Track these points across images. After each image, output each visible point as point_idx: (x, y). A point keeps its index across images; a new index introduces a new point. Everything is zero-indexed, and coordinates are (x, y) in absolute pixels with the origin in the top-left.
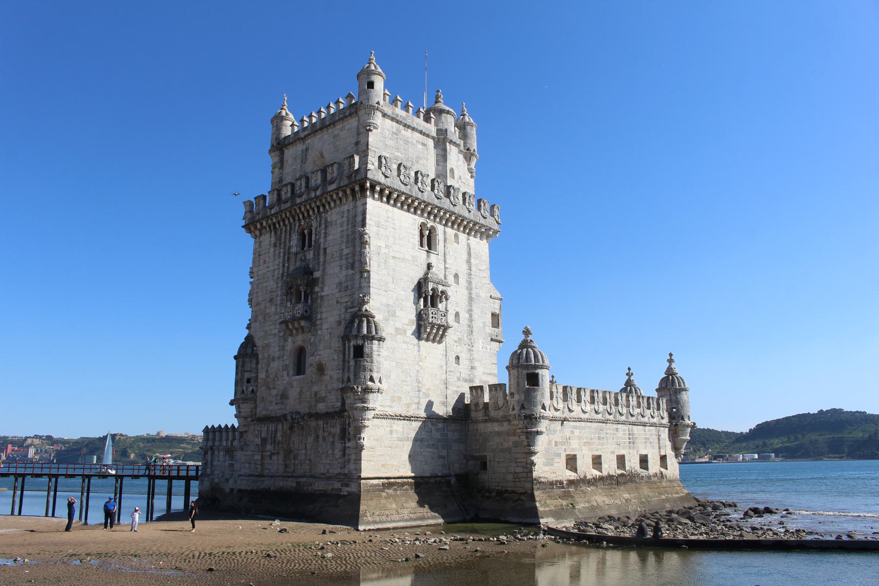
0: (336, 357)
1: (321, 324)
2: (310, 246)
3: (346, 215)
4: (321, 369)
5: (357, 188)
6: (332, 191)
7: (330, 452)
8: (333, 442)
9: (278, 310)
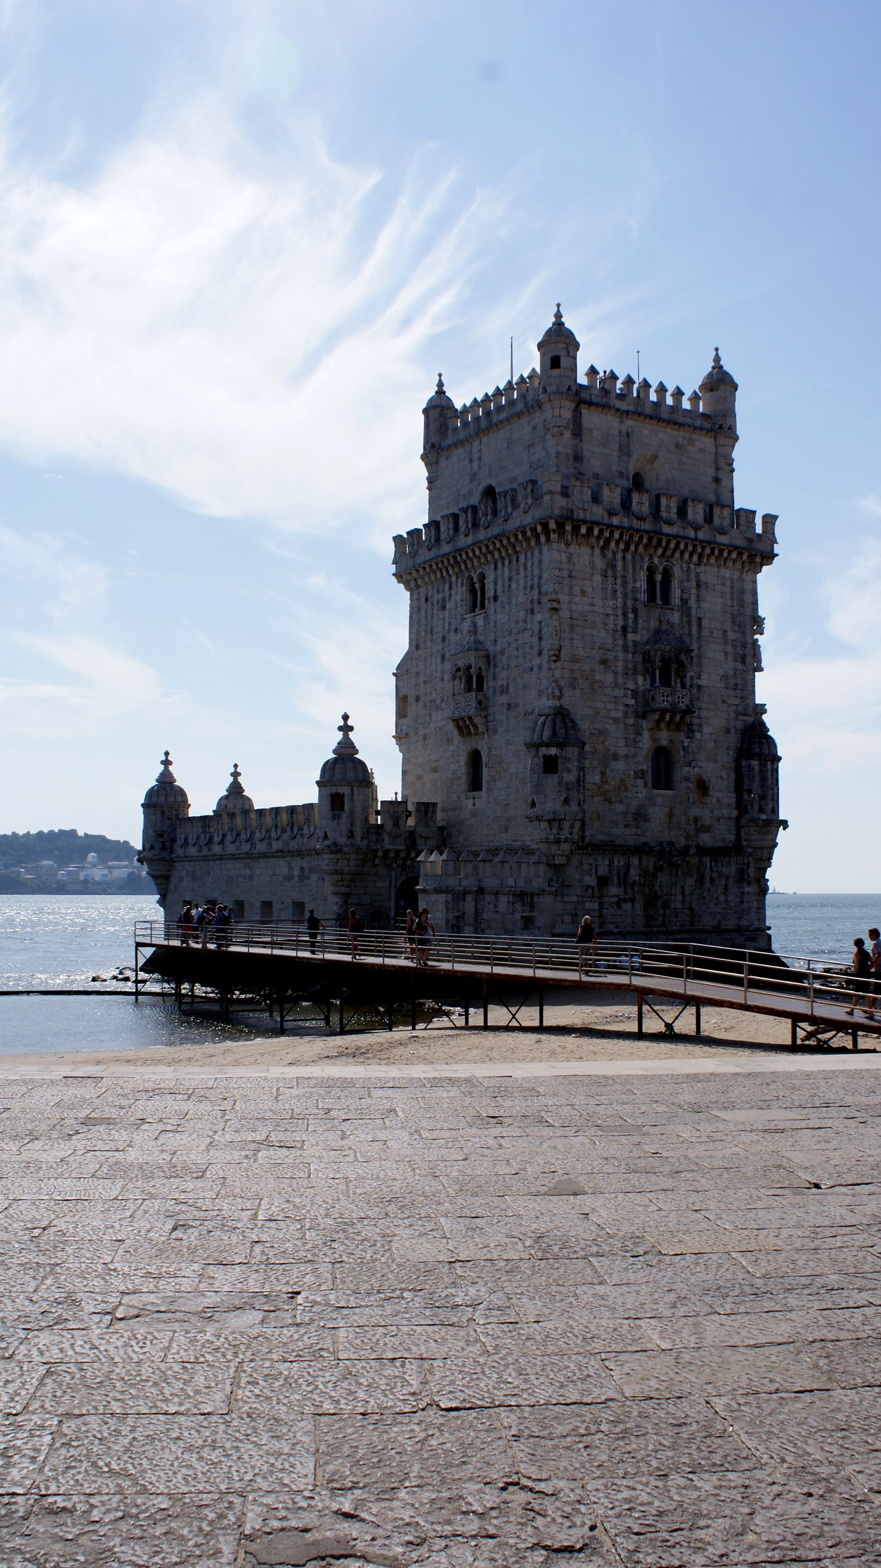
0: (724, 775)
1: (700, 725)
2: (666, 600)
3: (728, 584)
4: (703, 787)
5: (758, 560)
6: (728, 546)
7: (722, 898)
8: (726, 887)
9: (621, 681)
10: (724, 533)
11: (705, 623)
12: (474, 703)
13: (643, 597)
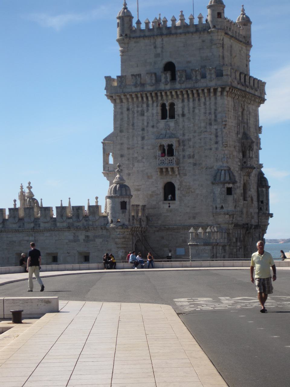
4: (252, 200)
9: (238, 155)
10: (256, 91)
11: (251, 128)
12: (175, 162)
13: (240, 118)
